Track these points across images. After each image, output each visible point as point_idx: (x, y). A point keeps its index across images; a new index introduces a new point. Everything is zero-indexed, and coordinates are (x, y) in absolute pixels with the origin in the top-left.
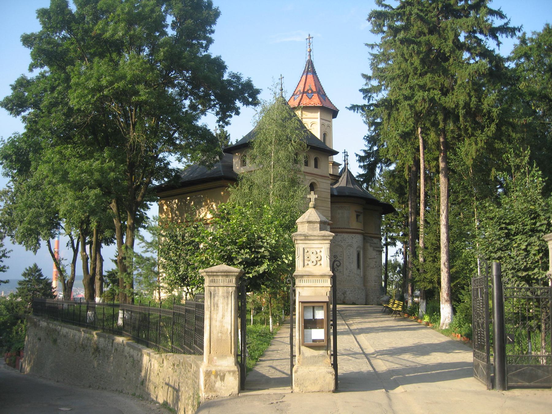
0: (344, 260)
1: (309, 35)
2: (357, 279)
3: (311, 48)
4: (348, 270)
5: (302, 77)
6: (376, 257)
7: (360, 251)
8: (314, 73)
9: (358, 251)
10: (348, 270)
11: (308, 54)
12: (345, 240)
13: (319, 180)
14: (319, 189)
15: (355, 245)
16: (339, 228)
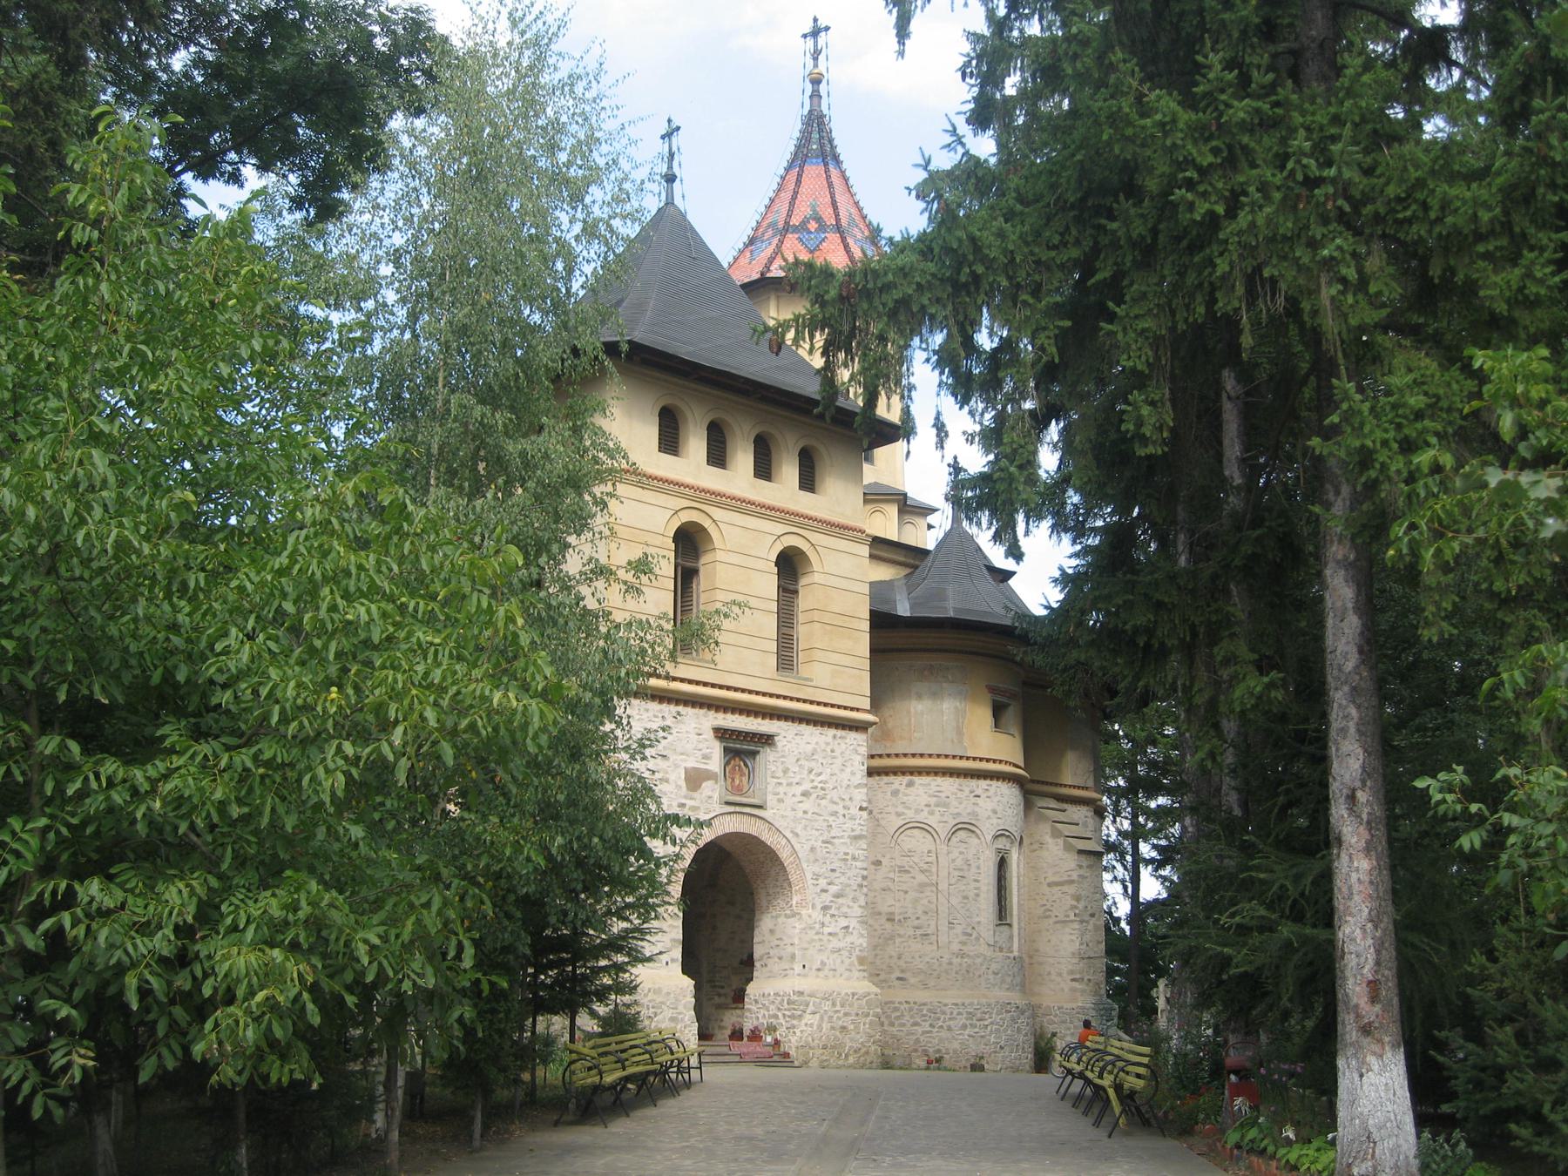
0: (943, 886)
1: (815, 20)
2: (994, 966)
3: (822, 68)
4: (959, 930)
5: (783, 178)
6: (1075, 876)
7: (1007, 852)
8: (829, 156)
9: (999, 851)
10: (959, 930)
11: (809, 88)
12: (946, 805)
14: (817, 578)
15: (989, 828)
16: (922, 755)
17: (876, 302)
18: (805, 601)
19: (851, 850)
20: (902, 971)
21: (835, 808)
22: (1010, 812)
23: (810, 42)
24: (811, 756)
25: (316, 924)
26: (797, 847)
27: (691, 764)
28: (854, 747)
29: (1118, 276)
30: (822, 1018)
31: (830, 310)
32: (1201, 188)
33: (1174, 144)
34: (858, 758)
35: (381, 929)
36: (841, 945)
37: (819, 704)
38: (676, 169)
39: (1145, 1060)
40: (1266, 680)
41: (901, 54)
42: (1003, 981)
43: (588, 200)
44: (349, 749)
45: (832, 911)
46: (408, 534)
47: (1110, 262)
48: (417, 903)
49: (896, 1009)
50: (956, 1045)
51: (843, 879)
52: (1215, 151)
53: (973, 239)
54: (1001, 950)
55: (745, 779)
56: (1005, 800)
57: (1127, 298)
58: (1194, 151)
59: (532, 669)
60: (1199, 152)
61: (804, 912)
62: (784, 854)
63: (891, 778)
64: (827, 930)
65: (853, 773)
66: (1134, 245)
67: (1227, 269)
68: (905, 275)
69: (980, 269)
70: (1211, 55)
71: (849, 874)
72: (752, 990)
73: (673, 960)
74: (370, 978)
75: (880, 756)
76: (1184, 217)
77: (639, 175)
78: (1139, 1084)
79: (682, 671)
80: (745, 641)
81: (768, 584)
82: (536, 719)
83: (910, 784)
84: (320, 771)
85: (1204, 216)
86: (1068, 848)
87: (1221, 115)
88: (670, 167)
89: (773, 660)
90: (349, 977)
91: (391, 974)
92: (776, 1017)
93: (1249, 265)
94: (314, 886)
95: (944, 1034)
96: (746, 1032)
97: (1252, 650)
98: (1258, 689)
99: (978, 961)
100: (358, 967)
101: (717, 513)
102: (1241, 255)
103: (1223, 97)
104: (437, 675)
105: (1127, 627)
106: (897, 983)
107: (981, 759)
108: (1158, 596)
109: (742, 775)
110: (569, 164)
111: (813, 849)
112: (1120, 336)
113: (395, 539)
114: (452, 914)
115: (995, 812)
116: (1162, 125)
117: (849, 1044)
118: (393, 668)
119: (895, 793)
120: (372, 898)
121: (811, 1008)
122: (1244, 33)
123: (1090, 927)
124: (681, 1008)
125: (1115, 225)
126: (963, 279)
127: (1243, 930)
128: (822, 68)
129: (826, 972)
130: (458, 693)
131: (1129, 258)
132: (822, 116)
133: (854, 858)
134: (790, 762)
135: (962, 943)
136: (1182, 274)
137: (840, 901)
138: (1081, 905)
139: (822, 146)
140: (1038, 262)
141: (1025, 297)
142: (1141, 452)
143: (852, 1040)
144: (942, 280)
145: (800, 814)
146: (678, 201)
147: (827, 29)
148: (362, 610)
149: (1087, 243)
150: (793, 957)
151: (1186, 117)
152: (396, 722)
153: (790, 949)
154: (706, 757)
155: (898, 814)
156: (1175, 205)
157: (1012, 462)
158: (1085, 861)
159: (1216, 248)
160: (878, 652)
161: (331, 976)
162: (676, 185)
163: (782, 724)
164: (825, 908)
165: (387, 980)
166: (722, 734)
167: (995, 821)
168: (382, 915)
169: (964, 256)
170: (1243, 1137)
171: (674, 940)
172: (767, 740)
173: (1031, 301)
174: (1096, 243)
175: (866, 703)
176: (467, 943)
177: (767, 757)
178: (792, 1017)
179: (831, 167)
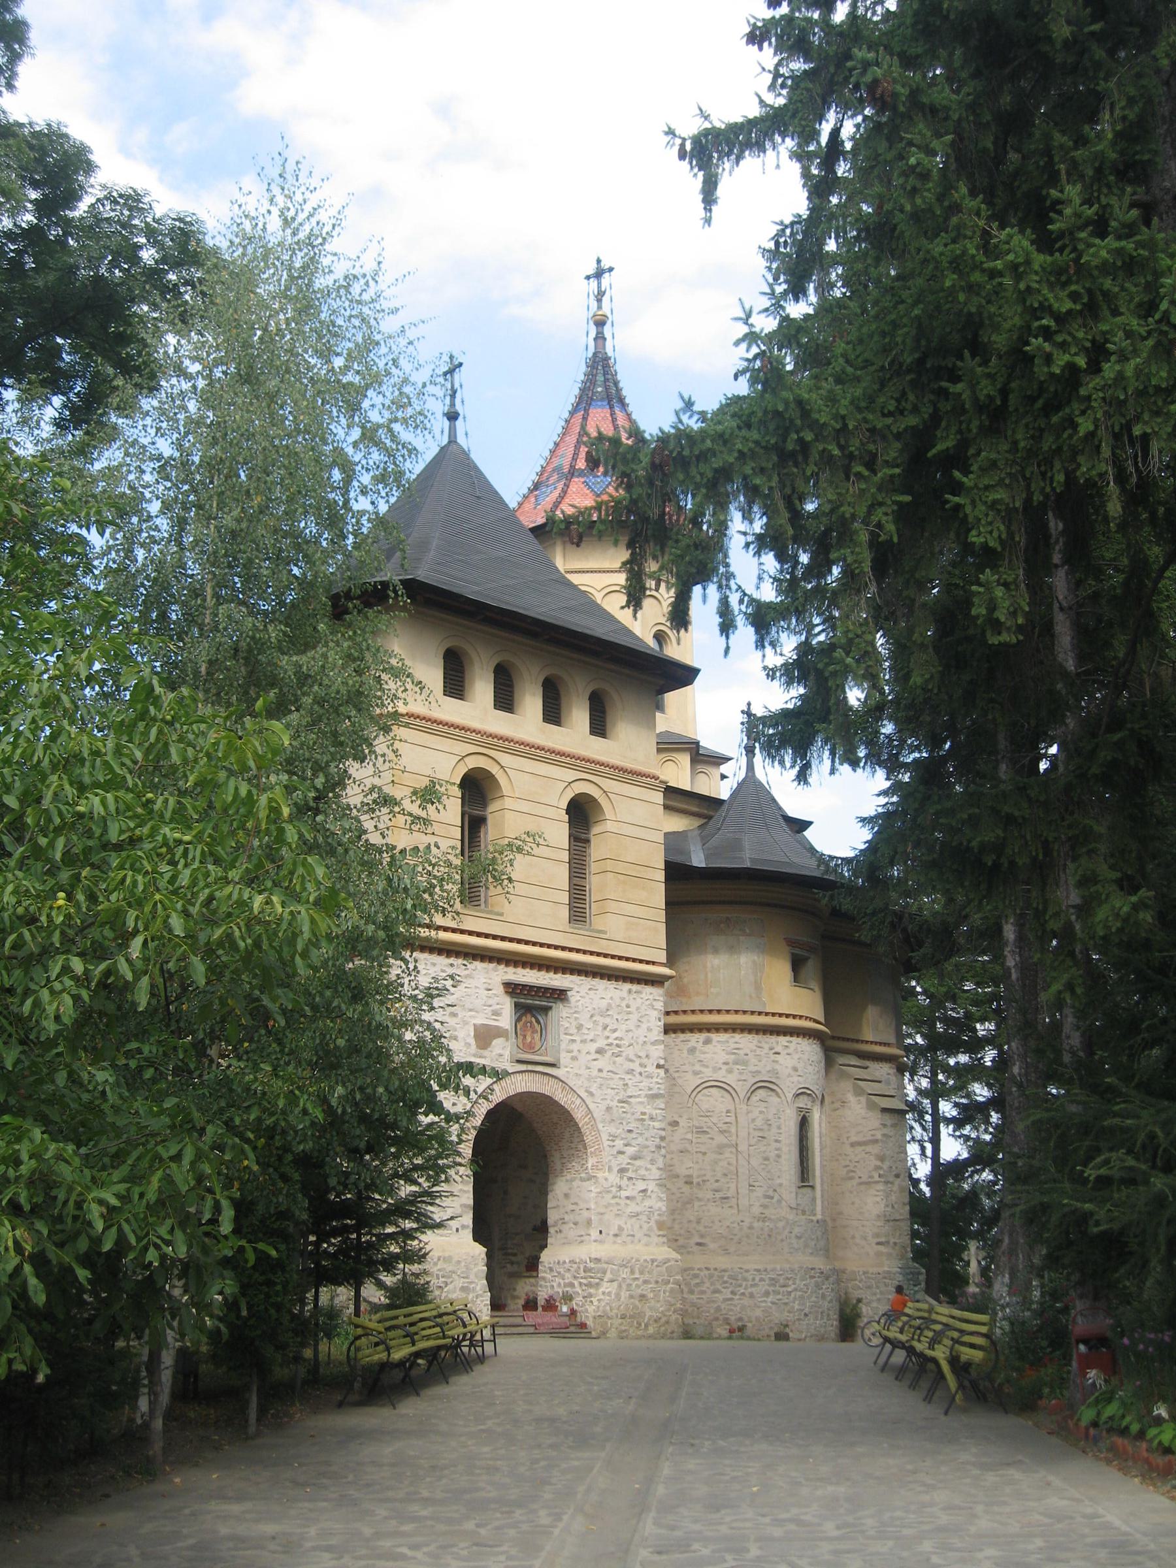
1: (599, 261)
2: (797, 1230)
3: (606, 309)
6: (879, 1137)
7: (808, 1111)
9: (800, 1109)
10: (759, 1192)
11: (593, 331)
12: (745, 1063)
13: (607, 784)
14: (609, 826)
15: (790, 1086)
16: (719, 1011)
17: (693, 471)
18: (598, 849)
19: (648, 1109)
20: (702, 1236)
21: (631, 1066)
22: (810, 1069)
23: (593, 283)
24: (605, 1013)
25: (43, 1182)
26: (592, 1106)
27: (480, 1021)
28: (651, 1000)
29: (963, 444)
30: (620, 1286)
31: (637, 491)
32: (1059, 338)
33: (1028, 288)
34: (655, 1014)
35: (121, 1188)
36: (638, 1209)
37: (613, 957)
38: (459, 407)
39: (984, 1329)
40: (1134, 899)
41: (708, 221)
42: (806, 1246)
43: (366, 404)
44: (78, 965)
45: (630, 1174)
46: (154, 719)
47: (954, 429)
48: (165, 1155)
49: (696, 1276)
50: (758, 1313)
51: (640, 1140)
52: (1074, 296)
53: (800, 403)
54: (804, 1213)
55: (537, 1036)
56: (806, 1057)
57: (974, 468)
58: (1050, 296)
59: (300, 870)
60: (1056, 297)
61: (600, 1175)
62: (578, 1115)
63: (688, 1036)
64: (624, 1194)
65: (649, 1030)
66: (980, 408)
67: (1091, 428)
68: (725, 442)
69: (809, 436)
70: (1068, 188)
71: (647, 1134)
72: (546, 1257)
73: (464, 1227)
74: (107, 1246)
75: (676, 1012)
76: (1041, 371)
77: (419, 378)
78: (978, 1355)
79: (470, 924)
80: (535, 892)
81: (559, 833)
82: (306, 928)
83: (707, 1042)
84: (45, 994)
85: (1063, 369)
86: (871, 1106)
87: (1080, 257)
88: (453, 404)
89: (565, 912)
90: (83, 1245)
91: (133, 1241)
92: (572, 1285)
93: (1117, 422)
94: (37, 1134)
95: (746, 1301)
96: (541, 1302)
97: (1112, 867)
98: (1125, 909)
99: (781, 1224)
100: (93, 1233)
101: (505, 759)
102: (1105, 413)
103: (1083, 235)
104: (184, 879)
105: (974, 844)
106: (696, 1248)
107: (780, 1015)
108: (1007, 809)
109: (534, 1032)
110: (346, 369)
111: (609, 1109)
112: (968, 509)
113: (141, 726)
114: (207, 1169)
115: (795, 1069)
116: (1014, 267)
117: (648, 1313)
118: (132, 868)
119: (692, 1051)
120: (113, 1150)
121: (609, 1276)
122: (1099, 171)
123: (895, 1188)
124: (472, 1277)
125: (959, 387)
126: (790, 446)
127: (1104, 1182)
128: (606, 309)
129: (624, 1237)
130: (211, 899)
131: (975, 425)
132: (607, 359)
133: (652, 1118)
134: (584, 1018)
135: (765, 1206)
136: (1037, 437)
137: (638, 1163)
138: (886, 1165)
139: (607, 389)
140: (873, 430)
141: (860, 469)
142: (994, 640)
143: (651, 1308)
144: (765, 448)
145: (595, 1073)
146: (461, 439)
147: (611, 269)
148: (97, 800)
149: (927, 411)
150: (589, 1222)
151: (1041, 257)
152: (136, 932)
153: (586, 1214)
154: (496, 1013)
155: (696, 1073)
156: (1029, 359)
157: (847, 654)
158: (889, 1119)
159: (1076, 405)
160: (672, 904)
161: (61, 1245)
162: (459, 423)
163: (575, 978)
164: (622, 1171)
165: (131, 1248)
166: (512, 989)
167: (796, 1079)
168: (124, 1170)
169: (792, 421)
170: (1099, 1414)
171: (463, 1206)
172: (560, 995)
173: (866, 473)
174: (936, 410)
175: (662, 957)
176: (225, 1203)
177: (560, 1012)
178: (589, 1285)
179: (617, 410)
